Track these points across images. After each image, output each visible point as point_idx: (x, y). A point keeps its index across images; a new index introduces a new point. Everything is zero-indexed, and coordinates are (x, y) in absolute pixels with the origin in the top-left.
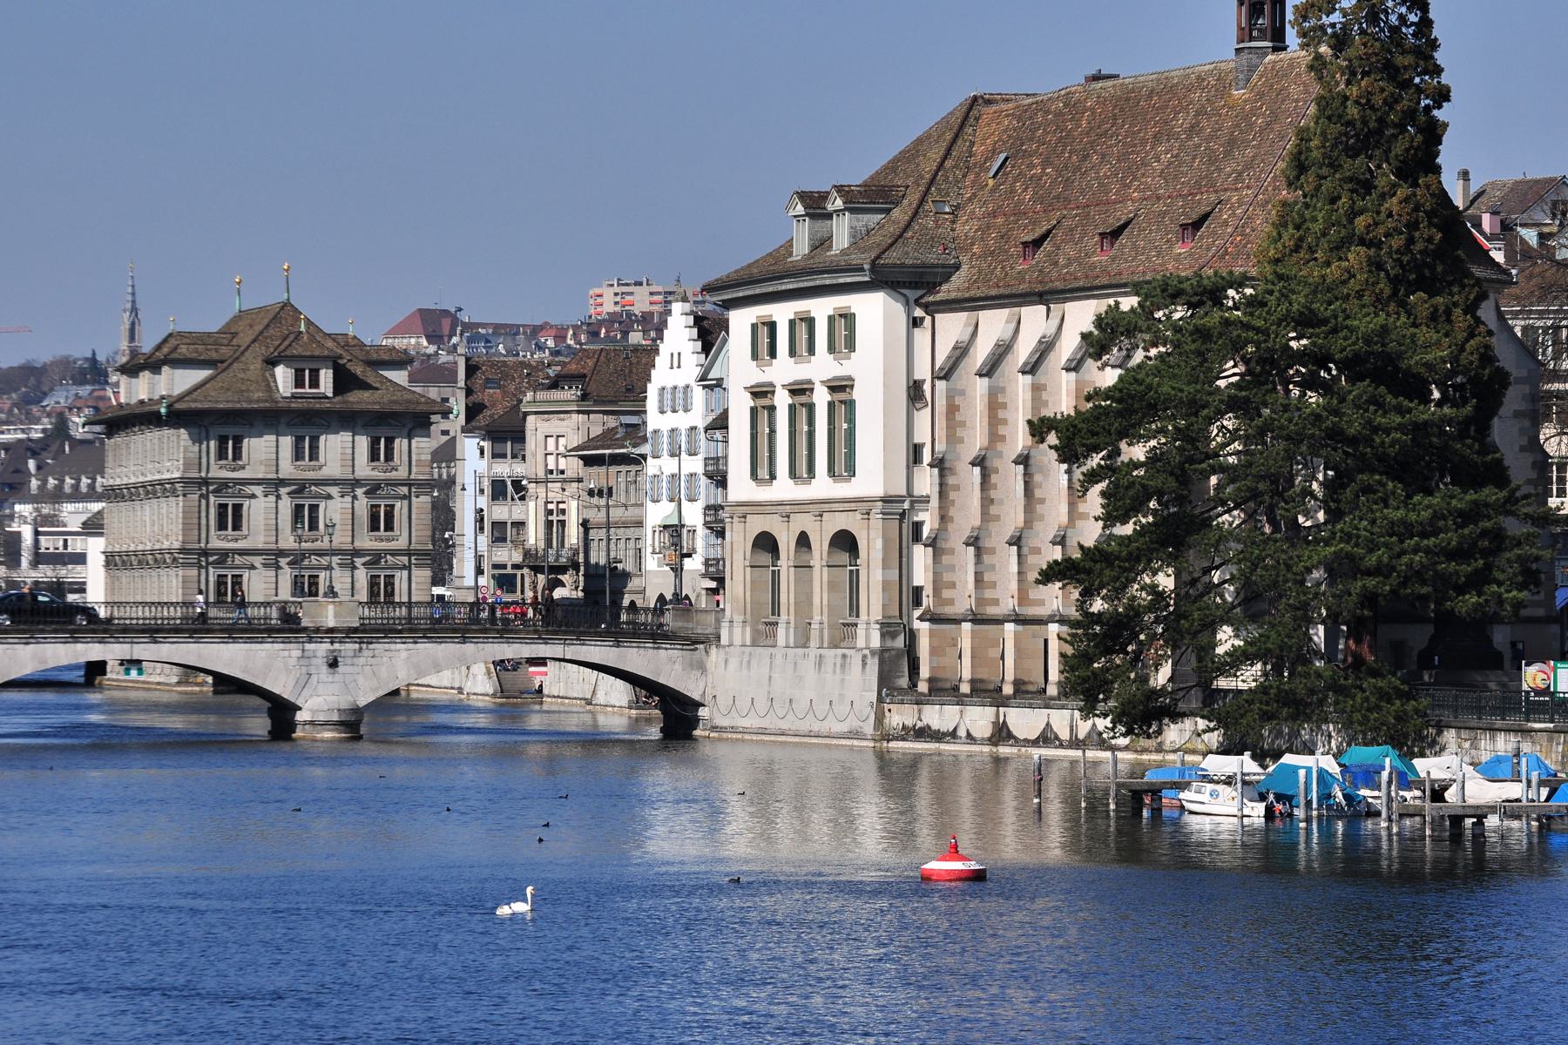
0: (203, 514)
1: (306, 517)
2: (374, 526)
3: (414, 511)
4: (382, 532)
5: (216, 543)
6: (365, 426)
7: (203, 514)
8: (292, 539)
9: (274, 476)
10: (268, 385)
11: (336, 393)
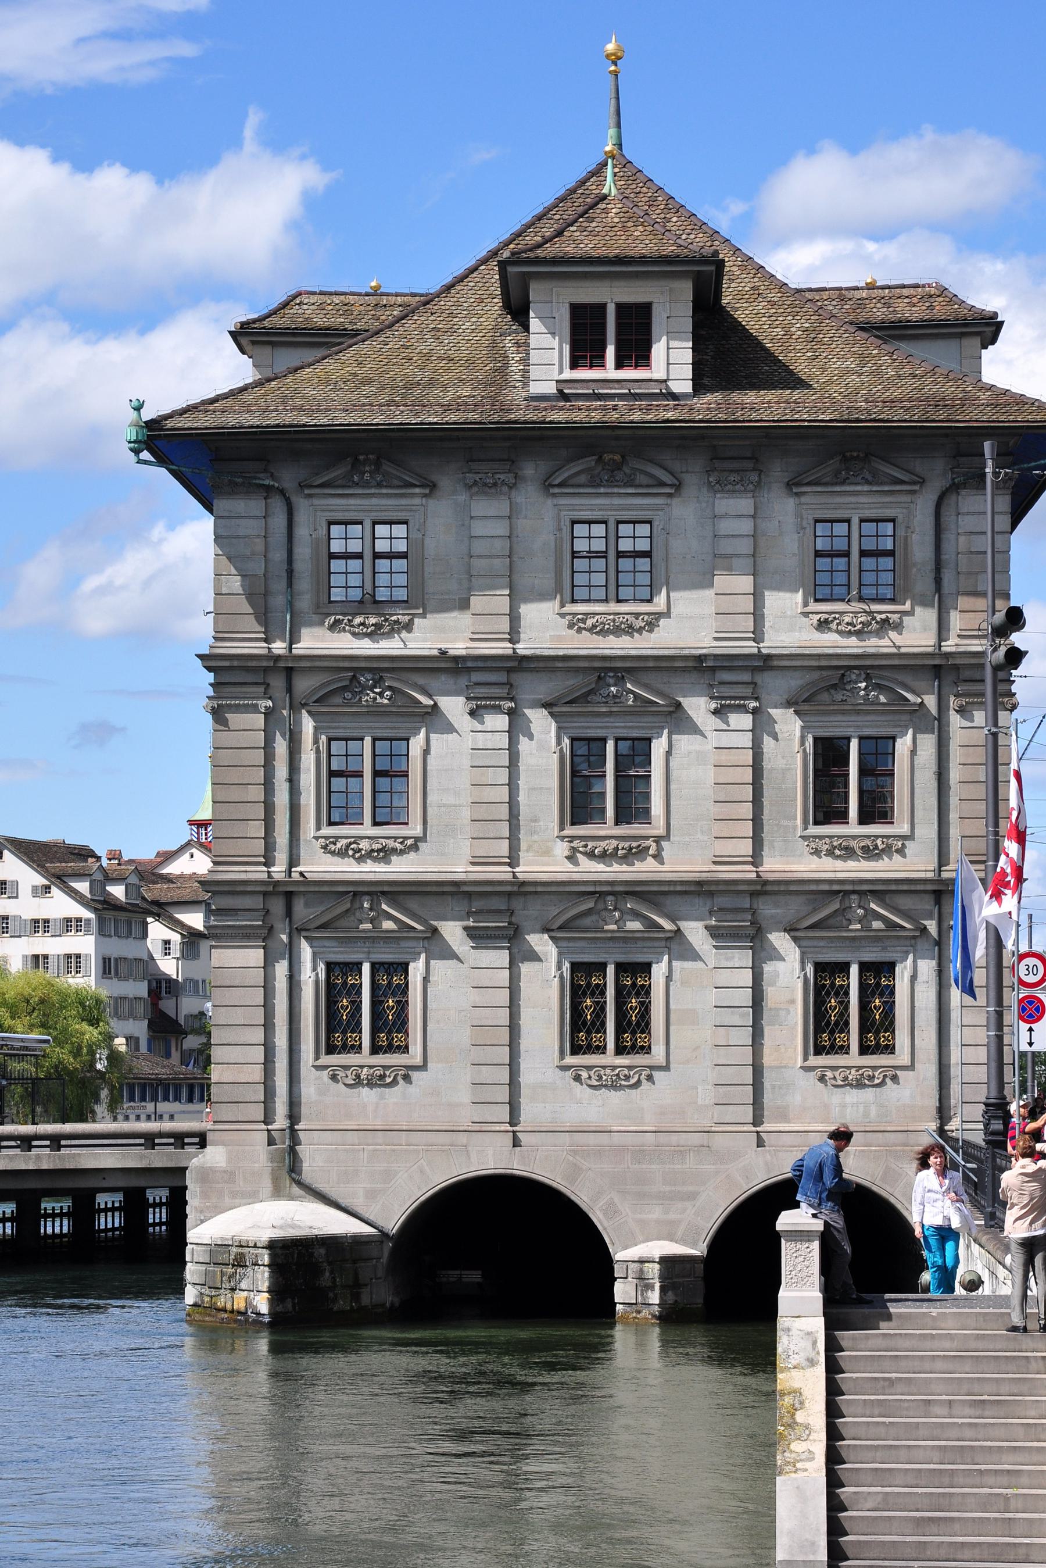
0: (281, 771)
1: (606, 782)
2: (827, 808)
3: (956, 755)
4: (853, 828)
5: (320, 866)
6: (793, 485)
7: (281, 771)
8: (562, 849)
9: (502, 648)
10: (502, 372)
11: (700, 385)
